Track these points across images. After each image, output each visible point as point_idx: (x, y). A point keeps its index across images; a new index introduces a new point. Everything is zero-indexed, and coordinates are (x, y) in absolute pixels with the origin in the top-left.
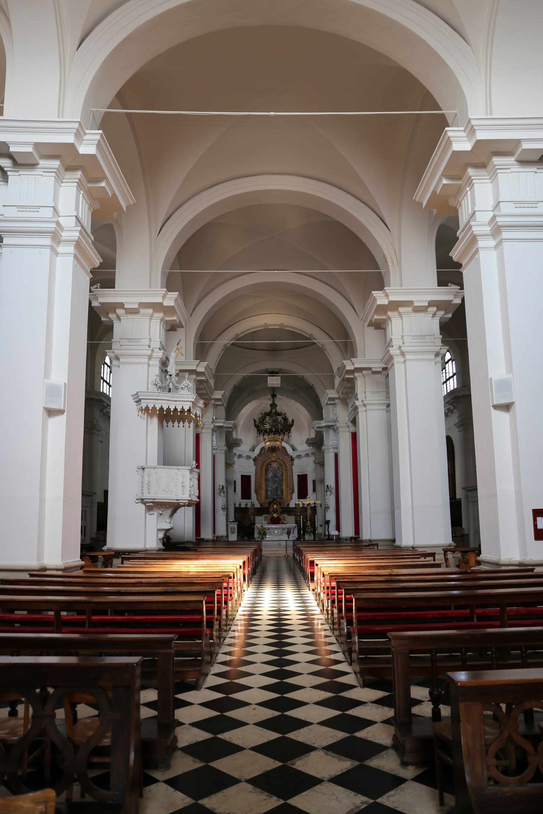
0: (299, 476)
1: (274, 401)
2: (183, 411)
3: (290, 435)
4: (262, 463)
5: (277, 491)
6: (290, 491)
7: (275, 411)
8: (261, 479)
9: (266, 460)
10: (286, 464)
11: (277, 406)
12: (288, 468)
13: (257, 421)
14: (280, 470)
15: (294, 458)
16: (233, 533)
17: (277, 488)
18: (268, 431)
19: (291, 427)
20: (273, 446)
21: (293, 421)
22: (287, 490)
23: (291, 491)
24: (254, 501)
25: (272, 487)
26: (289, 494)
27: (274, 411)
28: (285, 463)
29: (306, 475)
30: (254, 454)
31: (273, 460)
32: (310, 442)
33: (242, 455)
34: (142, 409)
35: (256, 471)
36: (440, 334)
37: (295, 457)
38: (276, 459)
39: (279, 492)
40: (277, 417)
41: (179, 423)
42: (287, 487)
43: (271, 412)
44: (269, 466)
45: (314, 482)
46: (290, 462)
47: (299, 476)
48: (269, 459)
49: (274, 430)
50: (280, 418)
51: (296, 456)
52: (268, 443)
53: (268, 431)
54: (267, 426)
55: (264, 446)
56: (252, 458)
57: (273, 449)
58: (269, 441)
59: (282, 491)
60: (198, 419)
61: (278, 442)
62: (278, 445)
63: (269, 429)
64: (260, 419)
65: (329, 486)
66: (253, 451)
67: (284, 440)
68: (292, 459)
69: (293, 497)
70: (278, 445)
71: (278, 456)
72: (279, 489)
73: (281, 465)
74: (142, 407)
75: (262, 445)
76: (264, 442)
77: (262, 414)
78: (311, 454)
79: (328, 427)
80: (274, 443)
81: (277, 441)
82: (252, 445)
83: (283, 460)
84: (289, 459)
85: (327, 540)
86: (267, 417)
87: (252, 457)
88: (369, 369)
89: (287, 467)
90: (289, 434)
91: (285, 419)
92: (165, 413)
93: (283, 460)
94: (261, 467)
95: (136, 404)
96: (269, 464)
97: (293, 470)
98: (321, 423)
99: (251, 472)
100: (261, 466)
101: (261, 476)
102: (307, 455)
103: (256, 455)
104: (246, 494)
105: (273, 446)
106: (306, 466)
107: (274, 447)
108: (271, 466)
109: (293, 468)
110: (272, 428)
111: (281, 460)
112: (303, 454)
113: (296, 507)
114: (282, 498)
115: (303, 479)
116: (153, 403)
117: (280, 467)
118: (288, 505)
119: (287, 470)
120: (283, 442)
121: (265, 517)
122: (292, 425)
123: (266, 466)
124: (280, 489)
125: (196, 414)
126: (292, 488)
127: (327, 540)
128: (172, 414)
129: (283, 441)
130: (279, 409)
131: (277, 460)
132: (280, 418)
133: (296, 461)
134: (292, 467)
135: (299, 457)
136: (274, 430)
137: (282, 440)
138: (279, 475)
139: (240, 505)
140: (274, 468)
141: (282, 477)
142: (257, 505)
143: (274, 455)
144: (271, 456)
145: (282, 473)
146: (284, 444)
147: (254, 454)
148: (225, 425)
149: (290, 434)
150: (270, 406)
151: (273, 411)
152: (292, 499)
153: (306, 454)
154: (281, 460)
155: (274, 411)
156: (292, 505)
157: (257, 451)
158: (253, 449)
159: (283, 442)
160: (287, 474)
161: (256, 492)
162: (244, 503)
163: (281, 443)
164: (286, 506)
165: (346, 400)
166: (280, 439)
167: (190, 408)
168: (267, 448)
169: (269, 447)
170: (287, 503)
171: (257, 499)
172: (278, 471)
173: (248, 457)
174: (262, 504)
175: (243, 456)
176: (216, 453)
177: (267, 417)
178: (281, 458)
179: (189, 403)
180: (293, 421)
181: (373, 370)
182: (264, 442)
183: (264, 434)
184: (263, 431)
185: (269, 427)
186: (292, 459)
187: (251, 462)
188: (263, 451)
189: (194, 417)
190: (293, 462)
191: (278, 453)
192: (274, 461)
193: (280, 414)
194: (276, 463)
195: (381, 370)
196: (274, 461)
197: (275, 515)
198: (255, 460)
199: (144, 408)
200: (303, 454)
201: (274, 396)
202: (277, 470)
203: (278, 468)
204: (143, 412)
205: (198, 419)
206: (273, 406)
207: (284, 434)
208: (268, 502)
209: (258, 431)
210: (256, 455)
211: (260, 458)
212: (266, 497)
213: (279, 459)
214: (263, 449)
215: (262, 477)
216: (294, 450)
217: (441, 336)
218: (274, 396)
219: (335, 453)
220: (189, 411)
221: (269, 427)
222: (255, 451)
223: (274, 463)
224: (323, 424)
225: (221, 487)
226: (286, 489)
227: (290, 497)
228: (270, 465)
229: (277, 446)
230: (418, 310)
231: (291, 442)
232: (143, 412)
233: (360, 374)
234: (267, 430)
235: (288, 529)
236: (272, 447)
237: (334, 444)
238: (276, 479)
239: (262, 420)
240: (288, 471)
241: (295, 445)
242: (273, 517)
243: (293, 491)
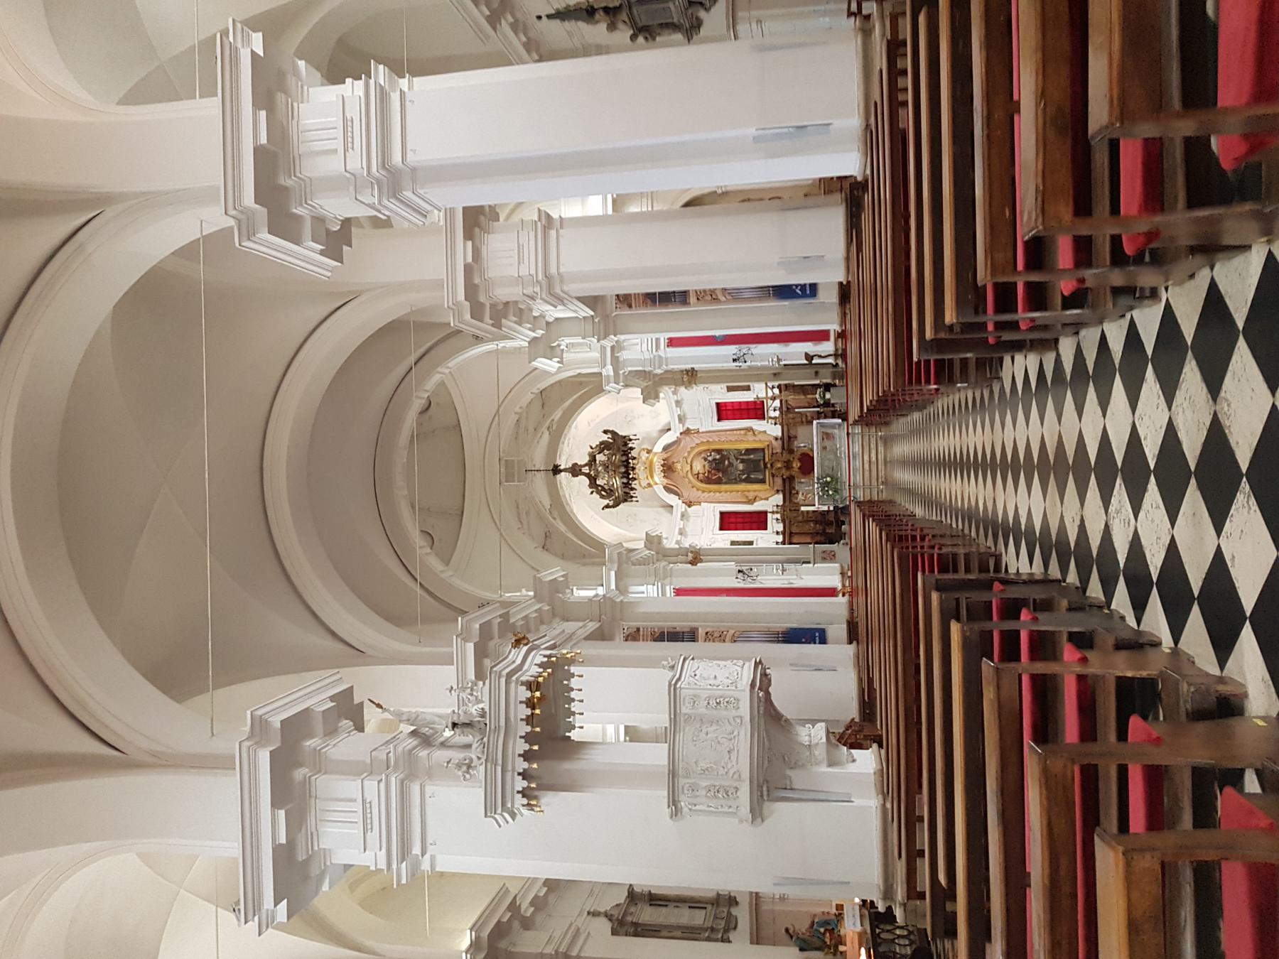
0: (719, 419)
1: (565, 470)
2: (530, 703)
3: (634, 438)
5: (749, 460)
6: (750, 437)
7: (587, 468)
9: (690, 482)
11: (576, 464)
12: (705, 440)
13: (606, 502)
15: (685, 429)
16: (834, 555)
17: (742, 461)
18: (625, 480)
19: (618, 434)
20: (662, 468)
21: (605, 432)
23: (748, 433)
24: (770, 502)
26: (754, 438)
27: (586, 470)
29: (718, 405)
30: (677, 505)
31: (689, 468)
32: (650, 395)
33: (680, 529)
34: (528, 804)
36: (344, 83)
39: (752, 456)
40: (597, 462)
41: (573, 700)
43: (588, 475)
44: (701, 475)
45: (730, 389)
46: (692, 436)
47: (719, 419)
48: (687, 477)
49: (623, 470)
50: (600, 458)
51: (681, 425)
52: (656, 479)
53: (625, 480)
54: (617, 482)
55: (661, 487)
56: (686, 510)
57: (668, 469)
58: (652, 477)
59: (748, 451)
60: (554, 659)
61: (655, 460)
63: (622, 478)
64: (602, 497)
65: (735, 357)
66: (672, 507)
67: (650, 448)
68: (687, 432)
71: (681, 459)
72: (745, 457)
73: (700, 453)
74: (523, 805)
76: (655, 487)
77: (592, 493)
78: (675, 397)
79: (616, 362)
81: (651, 462)
82: (662, 510)
83: (689, 449)
84: (687, 438)
85: (845, 360)
86: (598, 483)
87: (683, 510)
88: (468, 269)
89: (702, 442)
90: (630, 440)
91: (603, 446)
92: (536, 748)
93: (689, 449)
94: (703, 492)
95: (518, 817)
97: (707, 430)
98: (608, 376)
99: (714, 511)
100: (700, 492)
102: (678, 403)
103: (680, 501)
104: (757, 521)
105: (662, 468)
106: (699, 405)
109: (704, 430)
110: (620, 473)
111: (689, 453)
115: (723, 411)
116: (513, 776)
118: (776, 439)
119: (708, 441)
122: (613, 433)
123: (701, 481)
124: (745, 454)
125: (540, 666)
126: (742, 432)
127: (845, 360)
128: (538, 729)
129: (651, 451)
130: (586, 459)
131: (689, 462)
132: (600, 458)
134: (703, 433)
136: (623, 470)
137: (649, 452)
138: (718, 457)
139: (778, 533)
140: (704, 466)
142: (778, 499)
143: (678, 466)
144: (681, 472)
145: (714, 450)
146: (658, 448)
148: (616, 566)
149: (631, 437)
150: (577, 476)
151: (588, 471)
152: (765, 432)
153: (677, 406)
154: (689, 453)
155: (586, 470)
157: (672, 499)
159: (655, 450)
161: (751, 502)
162: (774, 524)
163: (656, 453)
164: (780, 442)
165: (548, 324)
166: (647, 455)
167: (523, 684)
168: (666, 481)
169: (664, 476)
170: (774, 442)
171: (767, 499)
172: (710, 458)
173: (684, 516)
174: (775, 489)
175: (681, 526)
176: (671, 585)
177: (598, 483)
178: (686, 454)
179: (513, 685)
180: (605, 432)
181: (470, 260)
182: (655, 487)
183: (632, 489)
184: (627, 490)
185: (617, 479)
186: (687, 432)
189: (550, 670)
192: (691, 466)
193: (593, 459)
194: (694, 465)
195: (469, 243)
196: (691, 466)
197: (796, 465)
198: (690, 504)
199: (525, 801)
201: (556, 470)
202: (709, 461)
203: (705, 459)
204: (533, 802)
205: (554, 659)
206: (575, 471)
207: (632, 449)
209: (625, 500)
210: (680, 501)
211: (685, 495)
214: (667, 489)
216: (669, 429)
217: (349, 81)
218: (556, 470)
219: (668, 346)
220: (530, 686)
221: (617, 479)
222: (672, 504)
223: (694, 468)
224: (609, 370)
225: (741, 574)
227: (760, 437)
228: (698, 474)
229: (662, 462)
230: (280, 132)
231: (655, 435)
232: (533, 802)
233: (482, 290)
234: (623, 483)
235: (823, 439)
236: (664, 471)
237: (650, 349)
238: (727, 462)
239: (606, 492)
240: (711, 440)
241: (659, 428)
242: (800, 468)
243: (750, 429)
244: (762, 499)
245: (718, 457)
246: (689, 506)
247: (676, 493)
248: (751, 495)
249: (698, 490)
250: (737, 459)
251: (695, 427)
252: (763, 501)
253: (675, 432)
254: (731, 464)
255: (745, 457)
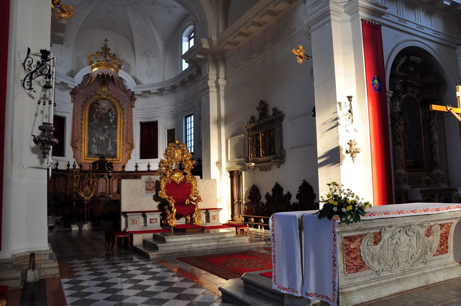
4: (86, 99)
8: (82, 124)
10: (122, 106)
14: (112, 113)
17: (107, 140)
22: (123, 145)
25: (99, 139)
26: (125, 150)
28: (121, 103)
30: (74, 82)
35: (74, 111)
37: (139, 95)
38: (107, 96)
42: (123, 140)
47: (142, 124)
52: (95, 69)
55: (90, 72)
56: (69, 88)
61: (112, 70)
62: (112, 73)
66: (73, 77)
69: (131, 156)
70: (112, 73)
71: (110, 92)
75: (86, 70)
80: (107, 70)
81: (111, 66)
82: (69, 69)
83: (118, 99)
84: (128, 98)
87: (69, 86)
93: (118, 99)
96: (95, 103)
97: (133, 114)
100: (83, 104)
101: (82, 119)
107: (107, 75)
108: (99, 106)
111: (115, 98)
112: (153, 90)
113: (136, 170)
114: (115, 156)
117: (112, 109)
118: (124, 167)
120: (120, 71)
121: (147, 182)
124: (112, 142)
131: (108, 98)
133: (139, 103)
134: (131, 110)
135: (146, 94)
138: (111, 121)
141: (116, 125)
143: (105, 89)
144: (100, 90)
146: (122, 74)
147: (74, 82)
156: (130, 167)
157: (79, 79)
158: (72, 74)
159: (120, 69)
160: (123, 119)
163: (118, 72)
168: (95, 76)
169: (98, 74)
172: (110, 114)
173: (63, 86)
178: (114, 96)
182: (90, 67)
187: (67, 96)
188: (89, 81)
190: (134, 103)
191: (110, 87)
194: (106, 102)
198: (74, 93)
200: (153, 90)
202: (107, 113)
203: (110, 110)
208: (92, 162)
211: (82, 92)
212: (90, 153)
213: (111, 96)
214: (88, 76)
215: (83, 123)
223: (103, 101)
226: (121, 143)
228: (98, 104)
236: (103, 75)
238: (106, 127)
241: (138, 78)
242: (173, 182)
243: (132, 147)
244: (74, 153)
245: (111, 121)
246: (71, 93)
247: (83, 82)
248: (78, 144)
249: (84, 102)
250: (109, 135)
251: (135, 106)
252: (73, 154)
253: (135, 88)
254: (104, 131)
255: (110, 141)
